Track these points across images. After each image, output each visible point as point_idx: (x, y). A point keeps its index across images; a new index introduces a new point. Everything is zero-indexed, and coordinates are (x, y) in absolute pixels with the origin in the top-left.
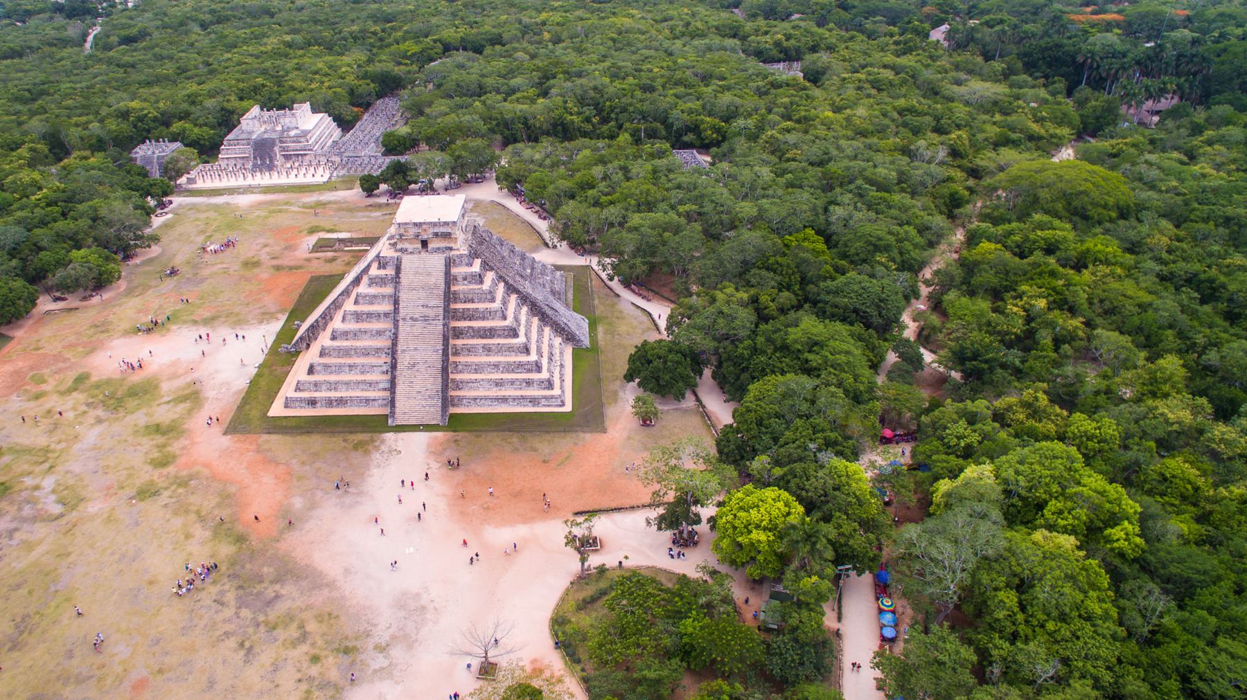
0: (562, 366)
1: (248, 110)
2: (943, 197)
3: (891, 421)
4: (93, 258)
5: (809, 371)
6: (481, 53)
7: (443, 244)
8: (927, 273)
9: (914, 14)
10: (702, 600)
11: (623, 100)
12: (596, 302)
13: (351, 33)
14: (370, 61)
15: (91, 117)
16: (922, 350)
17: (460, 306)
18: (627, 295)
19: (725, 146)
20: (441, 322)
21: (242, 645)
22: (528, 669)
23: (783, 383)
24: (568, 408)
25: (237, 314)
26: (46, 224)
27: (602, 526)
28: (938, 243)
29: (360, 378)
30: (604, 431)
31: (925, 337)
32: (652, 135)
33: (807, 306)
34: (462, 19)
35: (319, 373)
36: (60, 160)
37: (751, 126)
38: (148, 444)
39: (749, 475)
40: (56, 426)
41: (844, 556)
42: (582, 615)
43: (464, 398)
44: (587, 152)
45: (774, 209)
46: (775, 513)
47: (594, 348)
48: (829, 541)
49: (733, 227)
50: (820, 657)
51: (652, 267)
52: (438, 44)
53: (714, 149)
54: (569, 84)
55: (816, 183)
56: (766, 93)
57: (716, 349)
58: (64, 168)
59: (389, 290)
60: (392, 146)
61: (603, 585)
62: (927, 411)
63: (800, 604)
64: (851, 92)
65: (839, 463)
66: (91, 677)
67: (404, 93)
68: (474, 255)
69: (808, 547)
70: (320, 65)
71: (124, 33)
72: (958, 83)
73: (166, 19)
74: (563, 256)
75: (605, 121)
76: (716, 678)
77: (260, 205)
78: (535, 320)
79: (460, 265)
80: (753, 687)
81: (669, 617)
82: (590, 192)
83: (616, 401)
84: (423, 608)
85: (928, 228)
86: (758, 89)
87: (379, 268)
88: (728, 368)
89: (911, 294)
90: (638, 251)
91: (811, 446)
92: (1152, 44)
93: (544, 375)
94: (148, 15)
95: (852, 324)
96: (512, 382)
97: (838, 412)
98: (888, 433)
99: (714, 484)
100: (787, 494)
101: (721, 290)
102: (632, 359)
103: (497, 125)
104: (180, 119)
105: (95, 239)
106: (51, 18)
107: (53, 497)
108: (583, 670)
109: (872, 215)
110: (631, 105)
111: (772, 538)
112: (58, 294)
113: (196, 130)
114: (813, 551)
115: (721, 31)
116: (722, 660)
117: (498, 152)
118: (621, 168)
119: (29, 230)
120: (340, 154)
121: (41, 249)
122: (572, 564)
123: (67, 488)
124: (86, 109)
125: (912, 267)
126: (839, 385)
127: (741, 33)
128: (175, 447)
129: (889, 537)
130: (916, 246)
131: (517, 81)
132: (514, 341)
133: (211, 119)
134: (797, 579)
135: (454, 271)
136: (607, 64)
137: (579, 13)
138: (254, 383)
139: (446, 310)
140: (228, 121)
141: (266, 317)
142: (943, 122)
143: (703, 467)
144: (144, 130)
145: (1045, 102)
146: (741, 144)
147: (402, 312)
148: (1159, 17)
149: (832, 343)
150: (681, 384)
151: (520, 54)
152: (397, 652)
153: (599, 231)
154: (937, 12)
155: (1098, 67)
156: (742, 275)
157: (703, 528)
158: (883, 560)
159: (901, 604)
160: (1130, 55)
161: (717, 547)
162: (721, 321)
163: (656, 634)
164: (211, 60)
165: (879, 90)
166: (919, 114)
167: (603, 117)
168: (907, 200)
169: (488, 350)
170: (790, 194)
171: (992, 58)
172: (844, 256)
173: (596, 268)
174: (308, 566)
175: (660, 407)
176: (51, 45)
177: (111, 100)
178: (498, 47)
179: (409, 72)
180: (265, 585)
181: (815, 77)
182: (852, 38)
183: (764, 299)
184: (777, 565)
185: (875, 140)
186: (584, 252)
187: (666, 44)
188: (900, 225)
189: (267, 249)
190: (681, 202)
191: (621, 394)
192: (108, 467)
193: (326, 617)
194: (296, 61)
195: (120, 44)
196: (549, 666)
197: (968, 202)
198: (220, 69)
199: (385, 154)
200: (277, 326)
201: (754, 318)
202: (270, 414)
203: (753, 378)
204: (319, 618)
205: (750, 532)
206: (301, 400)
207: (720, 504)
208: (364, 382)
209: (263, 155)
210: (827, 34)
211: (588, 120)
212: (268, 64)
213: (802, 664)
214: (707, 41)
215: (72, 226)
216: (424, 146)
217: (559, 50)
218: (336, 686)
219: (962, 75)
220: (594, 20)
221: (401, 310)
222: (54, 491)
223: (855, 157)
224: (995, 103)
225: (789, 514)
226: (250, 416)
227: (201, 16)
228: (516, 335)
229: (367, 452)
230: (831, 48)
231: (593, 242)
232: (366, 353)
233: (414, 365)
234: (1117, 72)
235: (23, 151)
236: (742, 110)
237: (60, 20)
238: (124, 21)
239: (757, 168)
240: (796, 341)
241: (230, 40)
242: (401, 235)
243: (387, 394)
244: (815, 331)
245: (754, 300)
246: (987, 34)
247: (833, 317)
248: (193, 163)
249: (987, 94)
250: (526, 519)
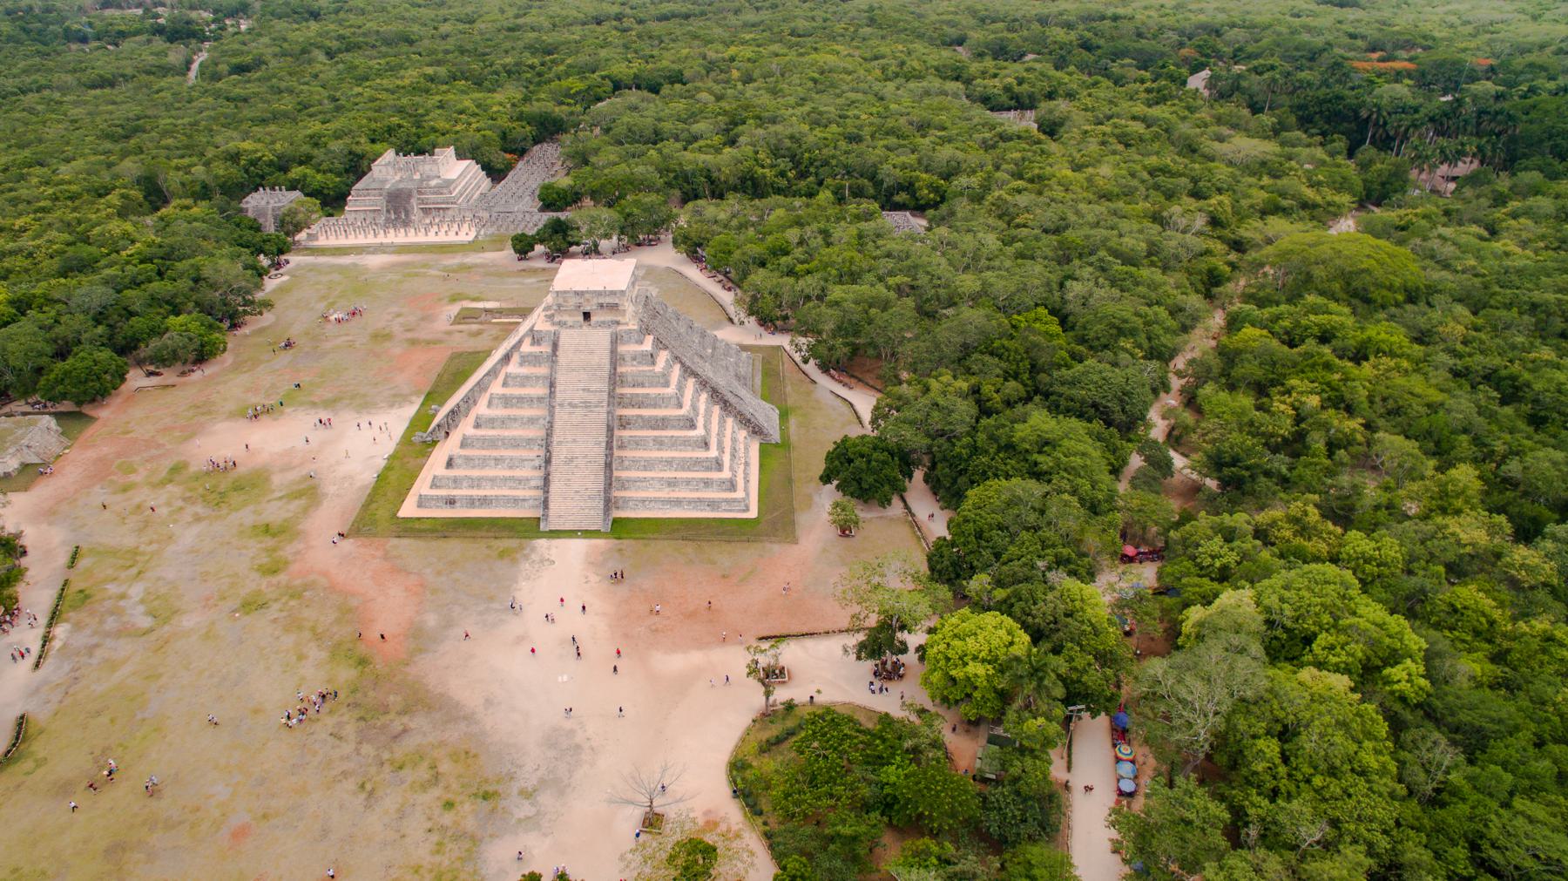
0: (747, 464)
1: (380, 155)
2: (1200, 273)
3: (1134, 536)
4: (194, 326)
5: (1037, 474)
6: (657, 92)
7: (609, 318)
8: (1180, 362)
9: (1170, 56)
10: (908, 744)
11: (825, 151)
12: (789, 389)
13: (504, 66)
14: (526, 100)
15: (195, 159)
16: (1172, 453)
17: (627, 391)
18: (824, 381)
19: (944, 208)
20: (605, 409)
21: (362, 786)
22: (701, 822)
23: (1009, 489)
24: (753, 513)
25: (365, 396)
26: (138, 285)
27: (790, 654)
28: (1193, 327)
29: (508, 473)
30: (795, 541)
31: (1176, 438)
32: (858, 193)
33: (1037, 398)
34: (636, 52)
35: (459, 467)
36: (157, 209)
37: (975, 185)
39: (965, 597)
40: (146, 524)
41: (1077, 695)
42: (766, 759)
43: (630, 499)
44: (780, 212)
45: (1001, 285)
46: (995, 643)
47: (786, 444)
48: (1059, 676)
49: (952, 303)
50: (1044, 813)
51: (855, 350)
52: (607, 82)
53: (930, 212)
54: (761, 131)
55: (1050, 254)
56: (994, 147)
57: (930, 447)
58: (162, 219)
59: (543, 370)
60: (552, 200)
61: (790, 723)
62: (1178, 525)
63: (1022, 751)
64: (1093, 147)
65: (1072, 584)
66: (180, 823)
67: (567, 138)
68: (645, 330)
69: (1034, 683)
70: (467, 103)
71: (234, 61)
72: (1221, 139)
73: (285, 45)
74: (749, 334)
75: (803, 175)
76: (923, 835)
77: (392, 267)
78: (717, 409)
79: (628, 342)
80: (965, 847)
81: (868, 763)
82: (784, 260)
83: (810, 506)
84: (578, 747)
85: (1181, 310)
86: (984, 141)
87: (533, 344)
88: (943, 470)
89: (1161, 387)
90: (839, 330)
91: (1040, 564)
92: (1449, 98)
93: (726, 474)
94: (266, 40)
95: (1090, 421)
96: (688, 482)
97: (1071, 524)
98: (1130, 550)
99: (924, 607)
100: (1010, 620)
101: (936, 378)
102: (830, 458)
103: (676, 178)
104: (301, 163)
105: (197, 304)
106: (149, 41)
107: (141, 608)
108: (765, 824)
109: (1116, 292)
110: (833, 157)
111: (991, 672)
112: (152, 368)
113: (319, 177)
114: (1039, 687)
115: (940, 72)
116: (930, 815)
117: (675, 211)
118: (821, 232)
119: (119, 292)
120: (489, 209)
121: (132, 314)
122: (753, 698)
123: (158, 597)
124: (189, 149)
125: (1162, 355)
126: (1074, 493)
127: (965, 76)
128: (288, 551)
129: (1129, 673)
130: (1167, 330)
131: (700, 127)
132: (692, 433)
133: (337, 165)
134: (1021, 721)
135: (622, 349)
136: (806, 108)
137: (775, 47)
138: (381, 478)
139: (611, 395)
140: (357, 167)
141: (397, 399)
142: (1201, 184)
143: (912, 586)
144: (257, 176)
145: (1323, 163)
146: (962, 207)
147: (559, 396)
148: (1457, 65)
149: (1066, 442)
150: (887, 488)
151: (704, 96)
152: (545, 799)
153: (794, 305)
154: (1197, 56)
155: (1385, 123)
156: (962, 360)
157: (910, 658)
158: (1122, 700)
159: (1142, 752)
160: (1423, 111)
161: (926, 681)
162: (935, 414)
163: (853, 783)
164: (338, 94)
165: (1127, 145)
166: (1173, 174)
167: (800, 172)
168: (1157, 275)
169: (660, 443)
170: (1019, 266)
171: (1261, 110)
172: (1082, 340)
173: (788, 348)
174: (442, 695)
175: (862, 515)
176: (149, 73)
177: (219, 139)
178: (678, 86)
179: (572, 113)
180: (392, 716)
181: (1051, 129)
182: (1095, 84)
183: (987, 389)
184: (998, 704)
185: (1121, 204)
186: (776, 330)
187: (877, 86)
188: (1149, 305)
189: (400, 320)
190: (891, 274)
191: (816, 498)
192: (207, 573)
193: (465, 756)
194: (438, 98)
195: (230, 74)
196: (724, 819)
197: (1229, 280)
198: (348, 105)
199: (542, 210)
200: (411, 410)
201: (974, 411)
202: (401, 514)
203: (972, 482)
204: (454, 757)
205: (965, 664)
206: (438, 498)
207: (931, 631)
208: (512, 479)
209: (398, 207)
210: (1066, 79)
211: (782, 174)
212: (404, 101)
213: (1024, 821)
214: (925, 84)
215: (169, 287)
216: (588, 202)
217: (750, 90)
218: (473, 838)
219: (1225, 131)
220: (792, 56)
221: (558, 395)
222: (142, 601)
223: (1097, 225)
224: (1264, 164)
225: (1011, 643)
226: (377, 515)
227: (328, 43)
228: (693, 426)
229: (514, 561)
230: (1070, 96)
231: (786, 318)
232: (515, 444)
233: (572, 460)
234: (1407, 130)
235: (113, 198)
236: (964, 166)
237: (159, 43)
238: (236, 46)
239: (980, 235)
240: (1023, 440)
241: (360, 71)
242: (559, 306)
243: (539, 493)
244: (1045, 427)
245: (976, 391)
246: (1254, 83)
247: (1068, 412)
248: (314, 216)
249: (1253, 153)
250: (700, 644)
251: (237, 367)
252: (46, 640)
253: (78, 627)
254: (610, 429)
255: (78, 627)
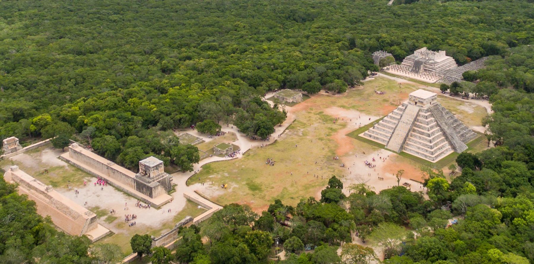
29: (385, 134)
38: (328, 131)
59: (401, 113)
169: (420, 138)
206: (368, 134)
232: (389, 128)
251: (346, 97)
252: (284, 131)
253: (290, 131)
254: (409, 131)
255: (290, 131)
